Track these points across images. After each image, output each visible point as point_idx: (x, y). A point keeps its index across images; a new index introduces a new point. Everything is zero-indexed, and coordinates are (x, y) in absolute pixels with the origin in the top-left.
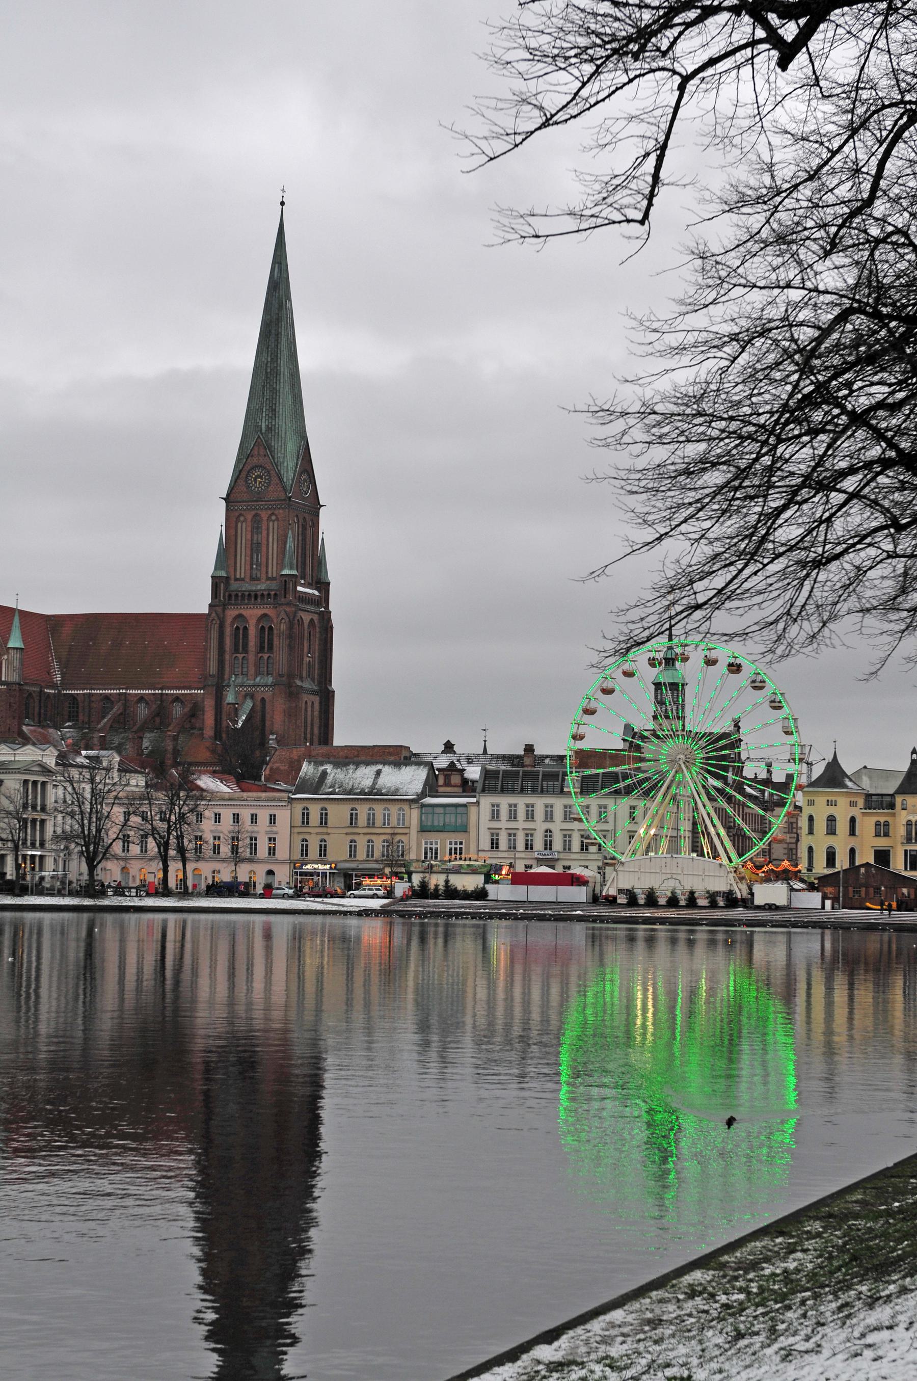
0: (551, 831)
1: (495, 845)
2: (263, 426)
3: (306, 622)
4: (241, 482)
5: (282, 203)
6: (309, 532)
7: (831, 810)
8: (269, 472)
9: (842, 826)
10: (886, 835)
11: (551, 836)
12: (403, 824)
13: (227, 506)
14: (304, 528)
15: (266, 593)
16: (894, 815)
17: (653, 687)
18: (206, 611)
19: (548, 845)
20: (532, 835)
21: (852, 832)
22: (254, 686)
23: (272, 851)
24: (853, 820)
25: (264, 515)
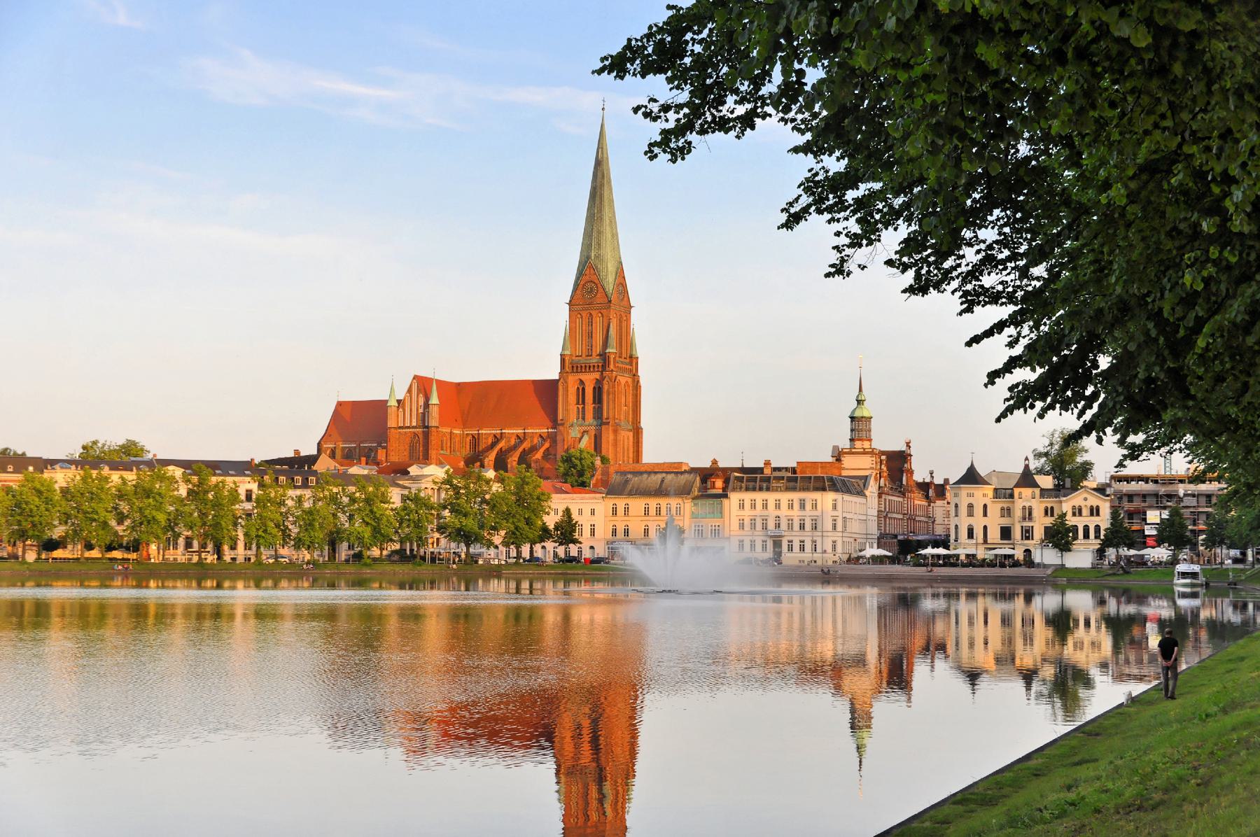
1: (742, 526)
3: (623, 384)
5: (603, 109)
6: (624, 324)
7: (971, 500)
9: (978, 510)
10: (1009, 515)
14: (621, 322)
16: (1013, 502)
18: (557, 378)
19: (778, 526)
20: (766, 520)
21: (985, 515)
23: (593, 533)
24: (985, 506)
25: (594, 313)
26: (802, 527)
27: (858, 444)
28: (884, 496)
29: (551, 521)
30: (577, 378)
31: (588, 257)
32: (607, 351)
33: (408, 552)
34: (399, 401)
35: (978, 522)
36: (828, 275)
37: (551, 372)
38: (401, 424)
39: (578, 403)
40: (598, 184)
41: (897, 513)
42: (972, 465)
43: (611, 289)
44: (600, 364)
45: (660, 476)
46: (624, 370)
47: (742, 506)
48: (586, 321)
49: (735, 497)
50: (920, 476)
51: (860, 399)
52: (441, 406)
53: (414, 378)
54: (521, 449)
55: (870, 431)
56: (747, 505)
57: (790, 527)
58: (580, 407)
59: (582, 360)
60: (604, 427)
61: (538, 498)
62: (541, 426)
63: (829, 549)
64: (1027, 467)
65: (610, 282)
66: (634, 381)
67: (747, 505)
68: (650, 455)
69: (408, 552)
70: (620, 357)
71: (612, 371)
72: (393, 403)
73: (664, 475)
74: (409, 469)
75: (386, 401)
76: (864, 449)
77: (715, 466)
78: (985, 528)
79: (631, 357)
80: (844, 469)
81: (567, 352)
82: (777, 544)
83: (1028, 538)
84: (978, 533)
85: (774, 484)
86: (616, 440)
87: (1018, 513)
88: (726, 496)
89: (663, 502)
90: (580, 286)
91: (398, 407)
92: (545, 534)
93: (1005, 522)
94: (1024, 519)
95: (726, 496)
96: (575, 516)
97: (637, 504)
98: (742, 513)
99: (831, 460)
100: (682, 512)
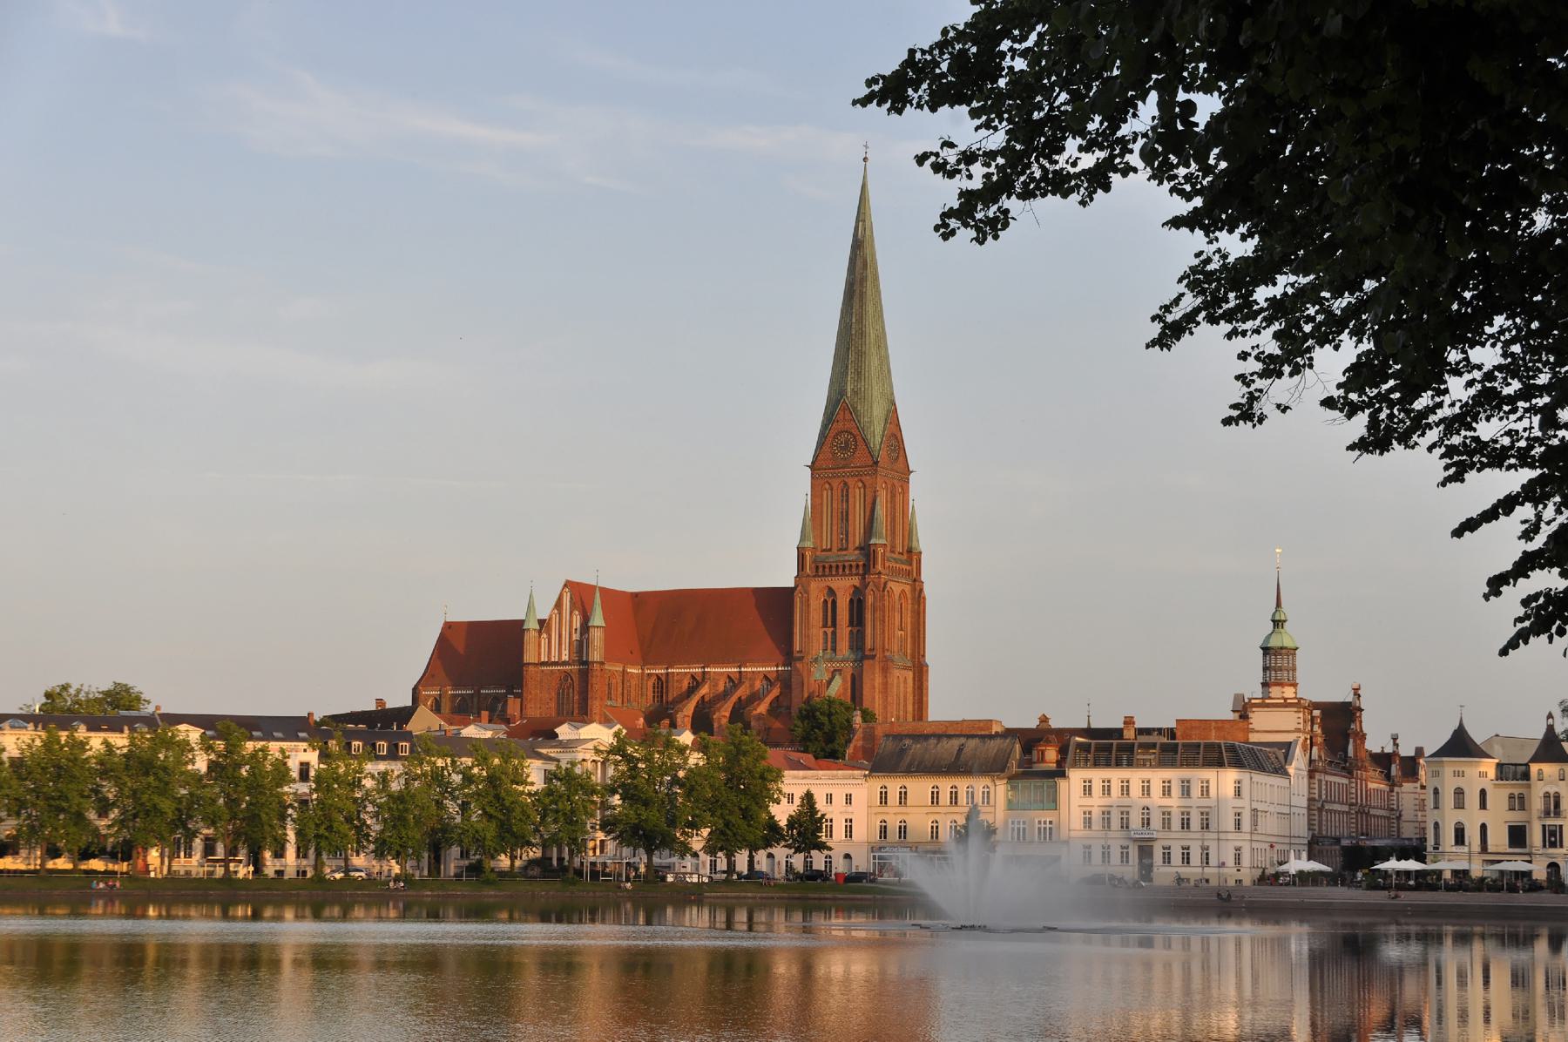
0: (1148, 809)
1: (1088, 822)
2: (849, 390)
4: (826, 448)
5: (865, 159)
6: (899, 499)
7: (1459, 782)
8: (855, 437)
9: (1472, 799)
10: (1522, 808)
11: (1148, 814)
12: (988, 803)
13: (812, 474)
14: (893, 496)
15: (854, 564)
16: (1529, 786)
17: (1262, 651)
18: (791, 584)
19: (1147, 823)
20: (1128, 813)
21: (1483, 806)
22: (842, 661)
23: (849, 831)
24: (1483, 793)
25: (851, 482)
26: (1186, 824)
27: (1275, 691)
28: (1317, 776)
29: (782, 812)
30: (823, 584)
31: (842, 393)
32: (872, 542)
33: (555, 862)
34: (541, 622)
35: (1472, 819)
36: (1227, 421)
37: (783, 575)
38: (544, 658)
39: (825, 625)
40: (858, 276)
41: (1339, 803)
42: (1461, 726)
43: (878, 439)
44: (861, 563)
45: (956, 743)
46: (898, 572)
47: (1088, 790)
48: (837, 493)
49: (1076, 776)
50: (1376, 742)
51: (1277, 618)
52: (606, 630)
53: (565, 586)
54: (734, 699)
55: (1294, 669)
56: (1097, 788)
57: (1167, 824)
58: (829, 631)
59: (833, 557)
60: (866, 663)
61: (762, 777)
62: (764, 663)
63: (1230, 861)
64: (1550, 728)
65: (876, 433)
66: (914, 590)
67: (1097, 788)
68: (943, 707)
69: (555, 862)
70: (893, 552)
71: (880, 573)
72: (532, 625)
73: (963, 740)
74: (557, 730)
75: (521, 622)
76: (1285, 699)
77: (1044, 726)
78: (1483, 827)
79: (910, 551)
80: (1253, 731)
81: (809, 544)
82: (1145, 851)
83: (1553, 845)
84: (1473, 836)
85: (1139, 755)
86: (885, 685)
87: (1537, 804)
88: (1063, 775)
89: (962, 784)
90: (829, 440)
91: (540, 632)
92: (773, 834)
93: (1517, 817)
94: (1547, 813)
95: (1063, 775)
96: (821, 805)
97: (920, 788)
98: (1087, 801)
99: (1231, 716)
100: (992, 802)
